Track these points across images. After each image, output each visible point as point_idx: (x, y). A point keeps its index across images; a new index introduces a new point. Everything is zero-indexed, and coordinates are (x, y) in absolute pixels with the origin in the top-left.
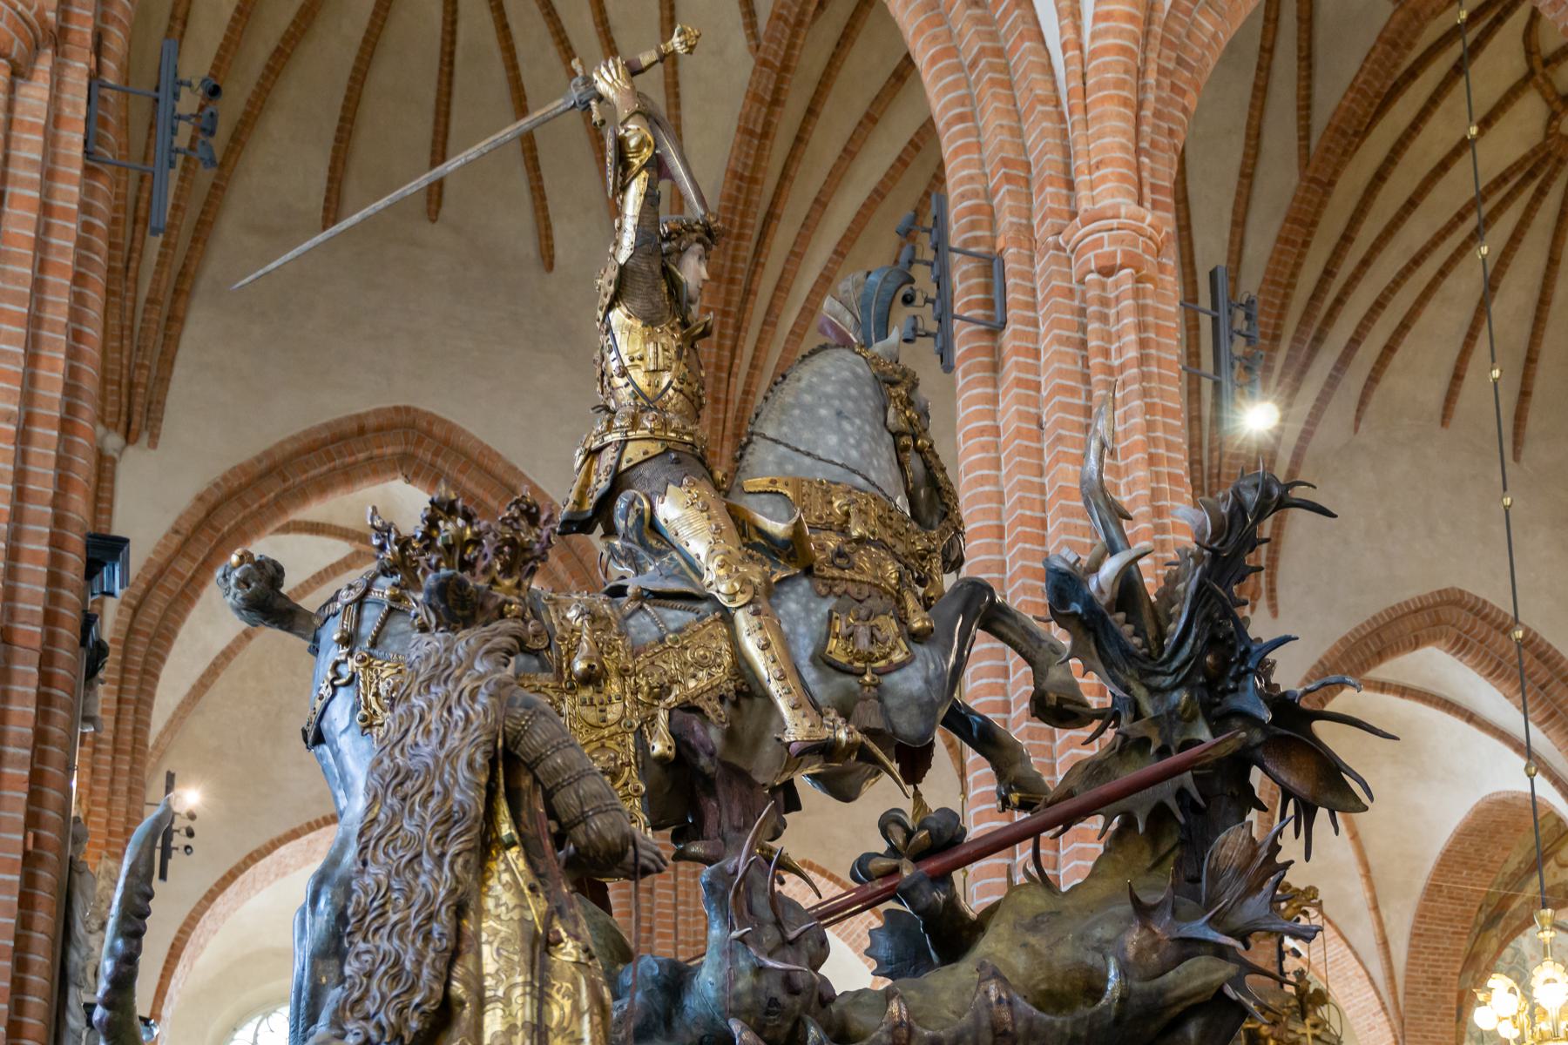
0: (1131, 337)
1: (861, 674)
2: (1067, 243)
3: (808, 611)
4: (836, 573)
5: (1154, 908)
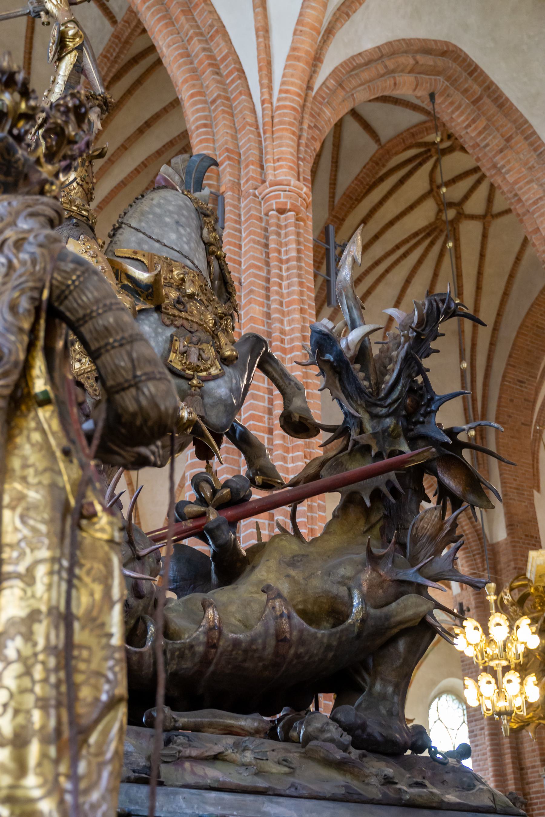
0: (293, 246)
1: (190, 379)
2: (260, 194)
3: (157, 334)
4: (176, 313)
5: (381, 557)
